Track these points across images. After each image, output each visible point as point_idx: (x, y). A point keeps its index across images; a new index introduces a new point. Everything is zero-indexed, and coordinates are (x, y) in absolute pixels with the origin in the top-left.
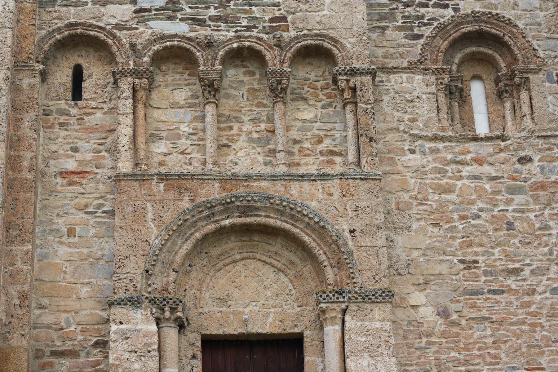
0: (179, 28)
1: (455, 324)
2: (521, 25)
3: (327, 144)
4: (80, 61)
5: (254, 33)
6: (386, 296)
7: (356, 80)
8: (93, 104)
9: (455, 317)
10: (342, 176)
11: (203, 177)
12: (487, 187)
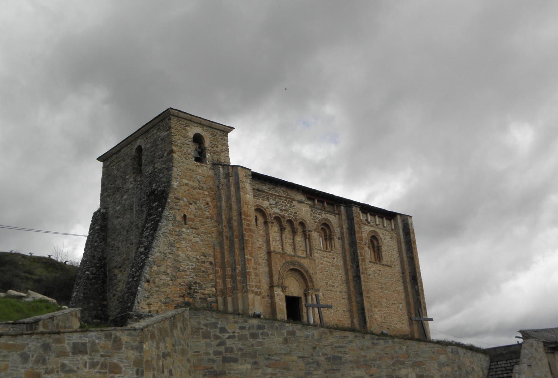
3: (302, 248)
5: (291, 216)
7: (310, 233)
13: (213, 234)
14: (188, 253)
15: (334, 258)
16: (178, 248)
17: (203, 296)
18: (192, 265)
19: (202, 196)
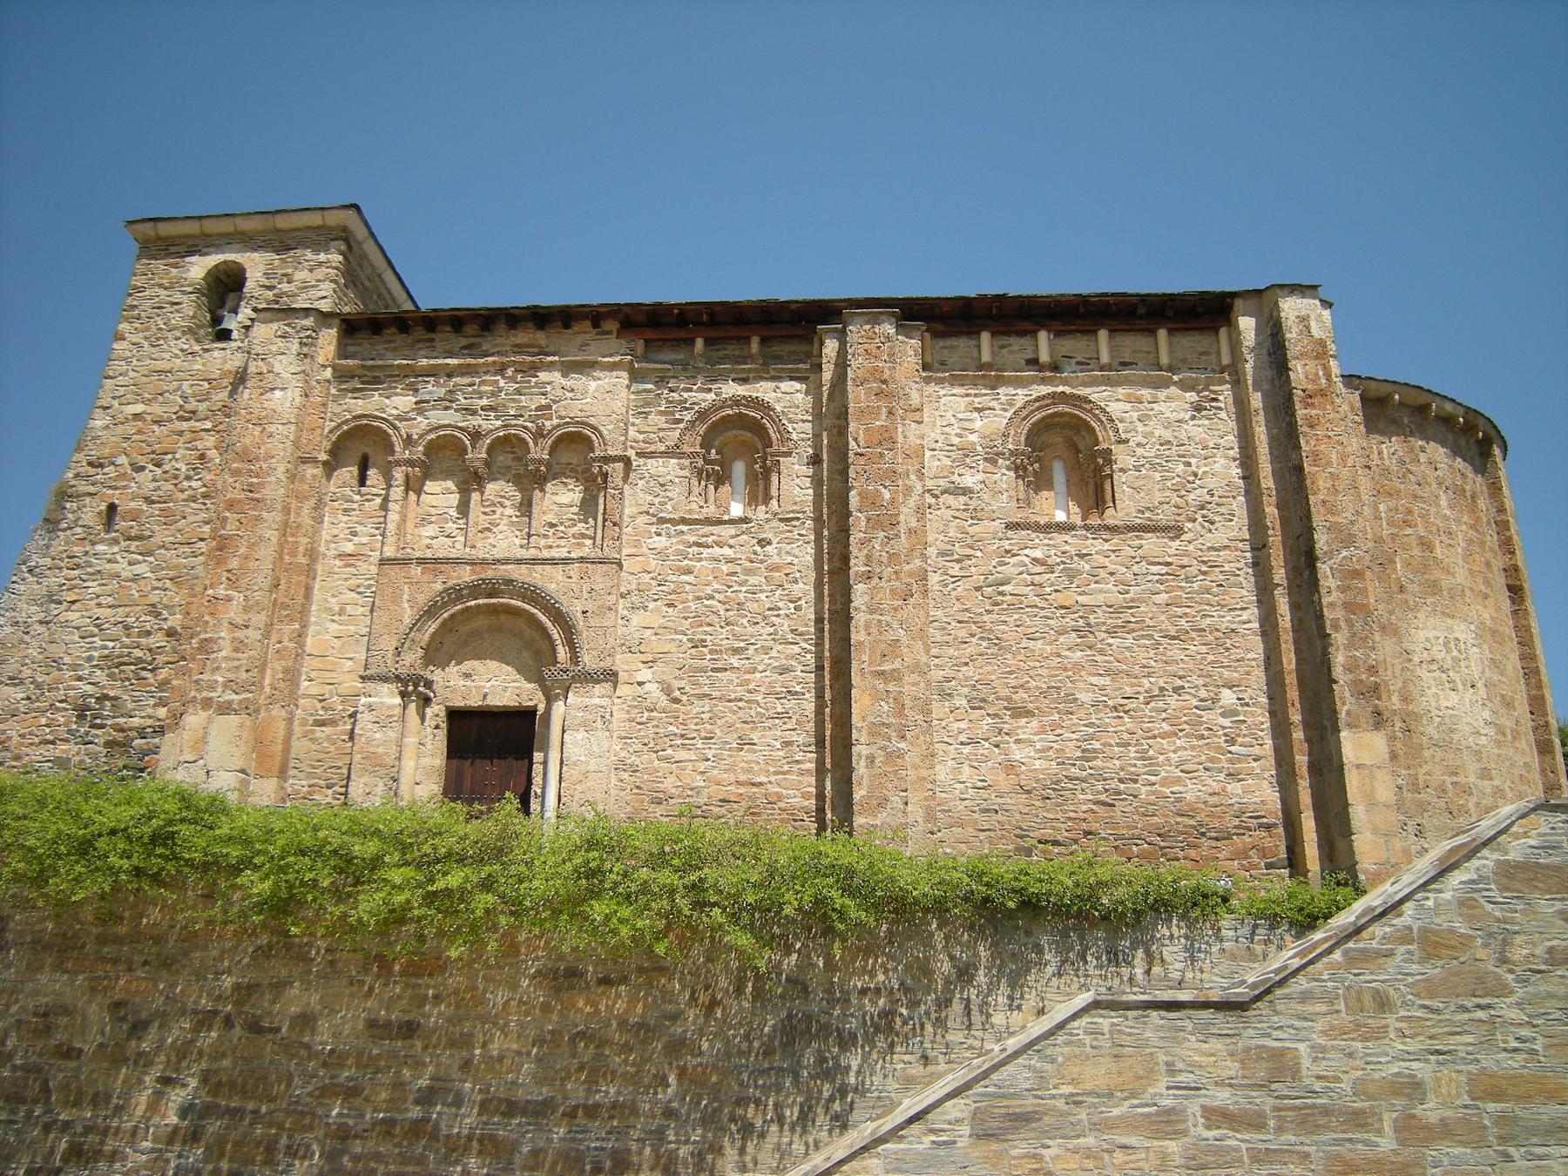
0: (450, 417)
1: (677, 701)
2: (778, 409)
4: (367, 450)
6: (611, 676)
8: (375, 491)
9: (677, 693)
10: (582, 560)
11: (457, 562)
12: (724, 568)
13: (202, 544)
14: (99, 612)
15: (763, 543)
16: (73, 602)
17: (120, 736)
18: (106, 647)
19: (188, 436)
